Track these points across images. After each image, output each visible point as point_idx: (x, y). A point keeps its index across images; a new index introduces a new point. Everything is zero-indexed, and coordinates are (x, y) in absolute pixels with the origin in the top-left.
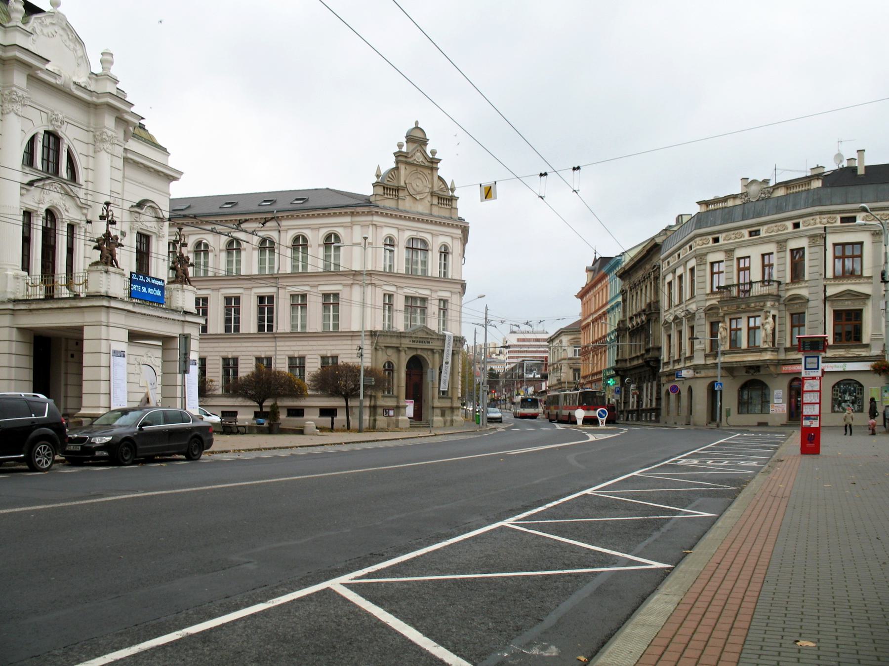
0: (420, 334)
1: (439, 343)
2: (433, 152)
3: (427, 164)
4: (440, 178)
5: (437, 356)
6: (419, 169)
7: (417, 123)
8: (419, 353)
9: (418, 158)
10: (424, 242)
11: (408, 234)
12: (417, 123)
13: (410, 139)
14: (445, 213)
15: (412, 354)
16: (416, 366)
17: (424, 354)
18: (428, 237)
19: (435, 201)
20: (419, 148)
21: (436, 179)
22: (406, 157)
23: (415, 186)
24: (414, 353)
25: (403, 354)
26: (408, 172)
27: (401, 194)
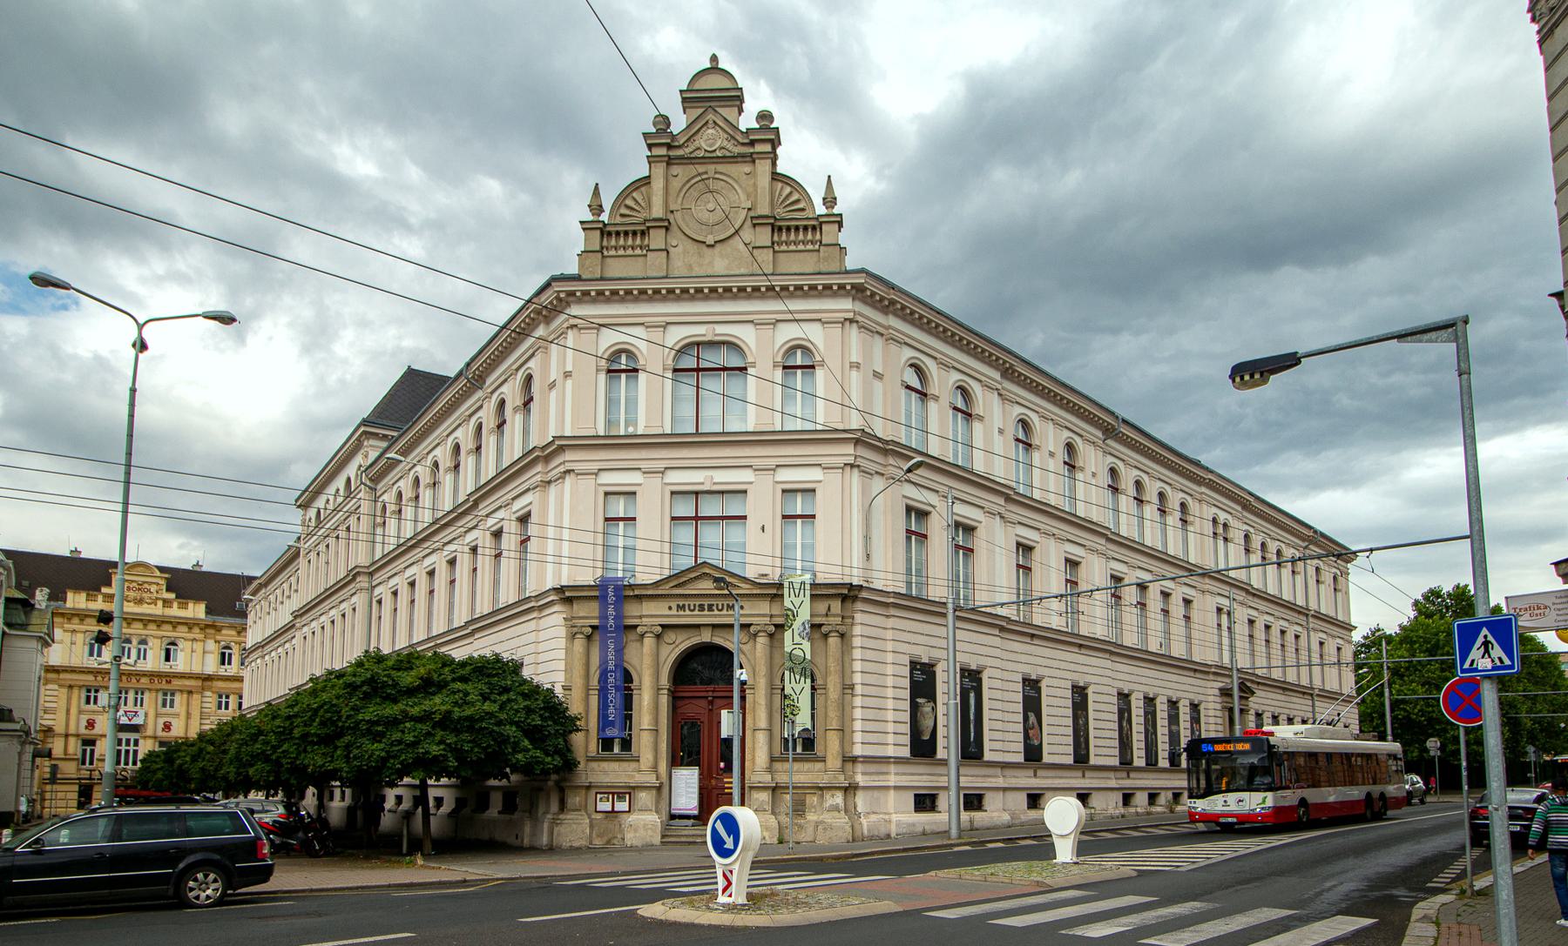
0: (706, 586)
1: (764, 607)
2: (765, 117)
3: (738, 150)
4: (776, 177)
5: (762, 640)
6: (711, 168)
7: (714, 58)
8: (706, 637)
9: (711, 140)
10: (733, 346)
11: (676, 336)
12: (714, 58)
13: (690, 99)
14: (798, 264)
15: (685, 642)
16: (703, 671)
17: (731, 642)
18: (746, 335)
19: (764, 236)
20: (710, 116)
21: (764, 180)
22: (669, 147)
23: (705, 216)
24: (695, 640)
25: (649, 641)
26: (676, 184)
27: (657, 239)
